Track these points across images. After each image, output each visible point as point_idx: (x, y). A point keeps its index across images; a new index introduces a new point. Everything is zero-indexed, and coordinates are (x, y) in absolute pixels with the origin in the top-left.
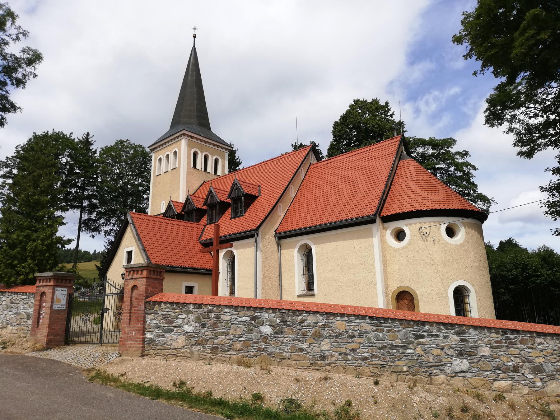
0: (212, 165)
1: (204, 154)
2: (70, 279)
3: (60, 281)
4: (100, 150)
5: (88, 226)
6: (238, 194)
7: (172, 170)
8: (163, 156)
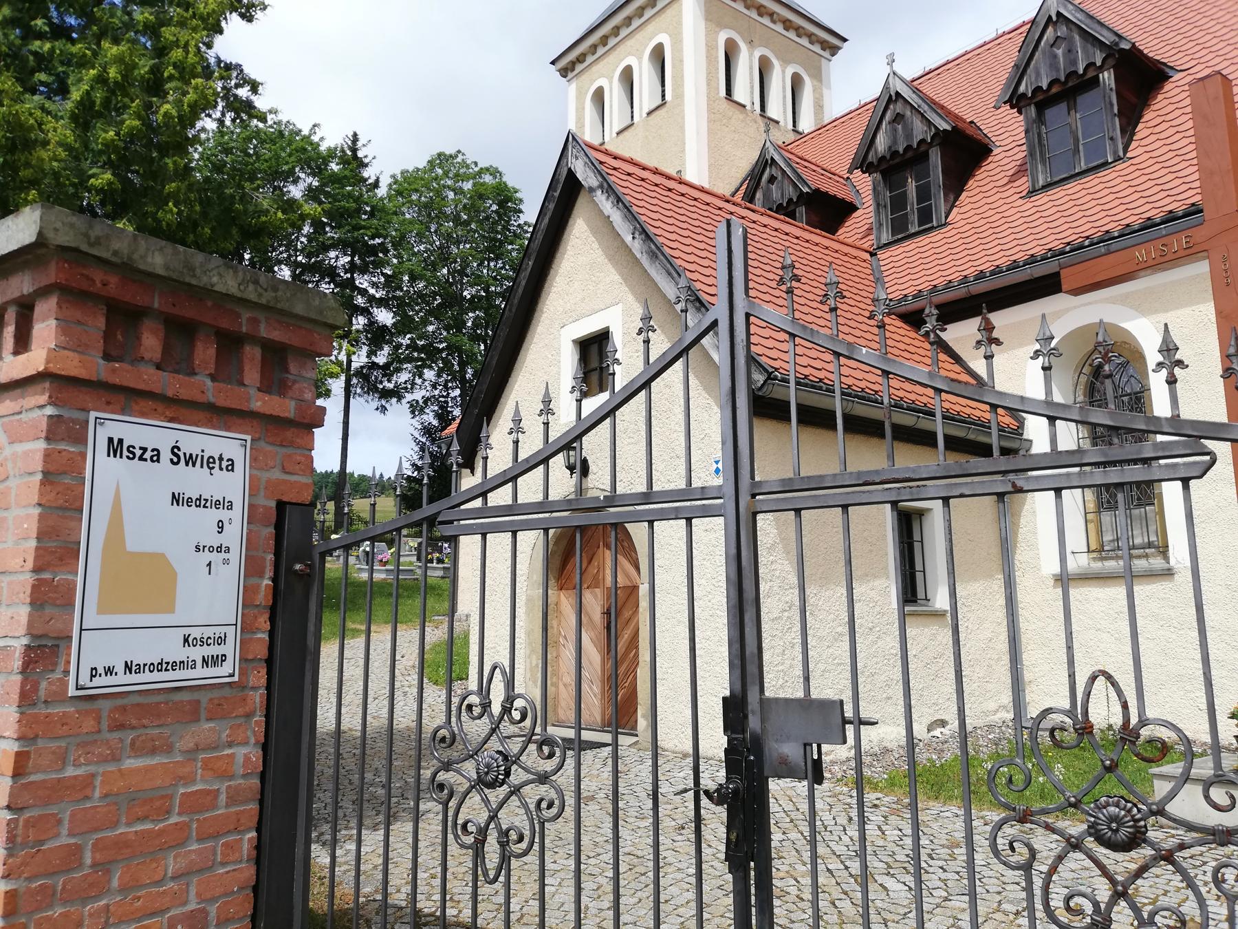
0: (784, 97)
1: (757, 54)
2: (277, 335)
3: (151, 342)
4: (390, 180)
5: (368, 382)
6: (1074, 62)
7: (649, 114)
8: (611, 83)
